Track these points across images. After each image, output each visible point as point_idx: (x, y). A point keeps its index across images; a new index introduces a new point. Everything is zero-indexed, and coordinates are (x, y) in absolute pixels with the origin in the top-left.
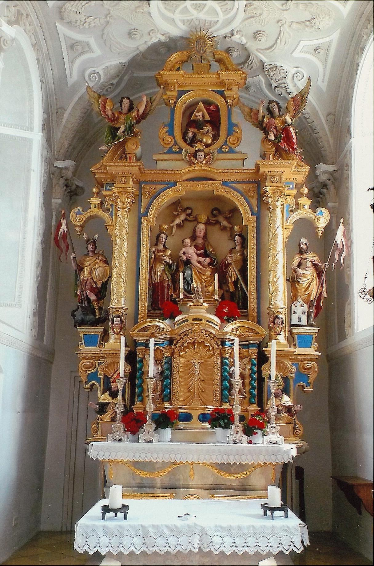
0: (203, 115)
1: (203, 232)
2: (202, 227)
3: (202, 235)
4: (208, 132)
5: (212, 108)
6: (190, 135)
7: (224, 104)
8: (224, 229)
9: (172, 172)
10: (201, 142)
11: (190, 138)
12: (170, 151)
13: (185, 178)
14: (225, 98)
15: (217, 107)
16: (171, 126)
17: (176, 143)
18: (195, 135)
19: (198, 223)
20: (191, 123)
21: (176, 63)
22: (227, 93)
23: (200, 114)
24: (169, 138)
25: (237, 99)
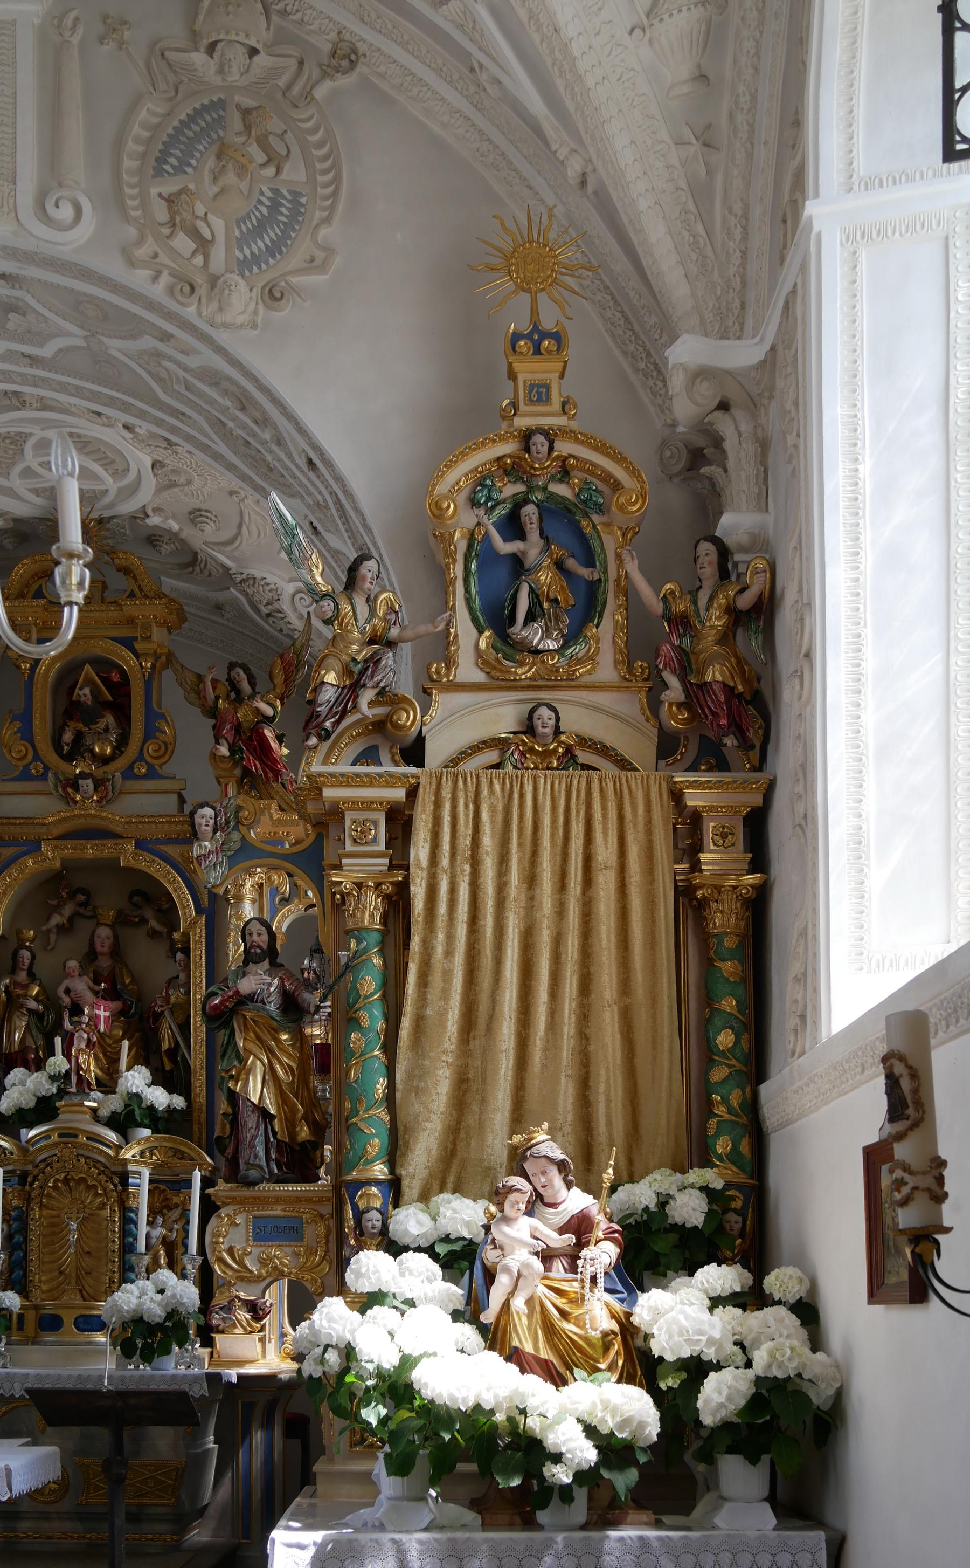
0: (95, 693)
1: (108, 943)
2: (104, 933)
3: (106, 950)
4: (107, 730)
5: (115, 677)
6: (68, 737)
7: (138, 668)
8: (154, 934)
9: (29, 821)
10: (92, 751)
11: (67, 744)
12: (25, 776)
13: (56, 832)
14: (137, 656)
15: (123, 672)
16: (26, 718)
17: (37, 757)
18: (79, 736)
19: (99, 924)
20: (69, 710)
21: (33, 577)
22: (138, 646)
23: (87, 691)
24: (21, 748)
25: (164, 658)
